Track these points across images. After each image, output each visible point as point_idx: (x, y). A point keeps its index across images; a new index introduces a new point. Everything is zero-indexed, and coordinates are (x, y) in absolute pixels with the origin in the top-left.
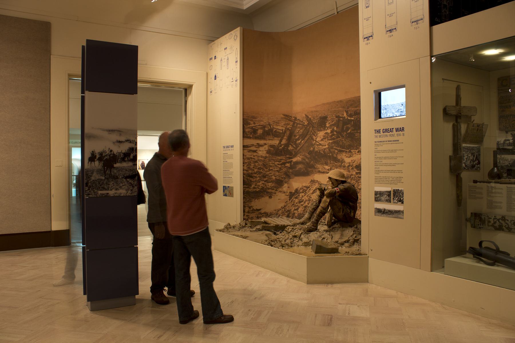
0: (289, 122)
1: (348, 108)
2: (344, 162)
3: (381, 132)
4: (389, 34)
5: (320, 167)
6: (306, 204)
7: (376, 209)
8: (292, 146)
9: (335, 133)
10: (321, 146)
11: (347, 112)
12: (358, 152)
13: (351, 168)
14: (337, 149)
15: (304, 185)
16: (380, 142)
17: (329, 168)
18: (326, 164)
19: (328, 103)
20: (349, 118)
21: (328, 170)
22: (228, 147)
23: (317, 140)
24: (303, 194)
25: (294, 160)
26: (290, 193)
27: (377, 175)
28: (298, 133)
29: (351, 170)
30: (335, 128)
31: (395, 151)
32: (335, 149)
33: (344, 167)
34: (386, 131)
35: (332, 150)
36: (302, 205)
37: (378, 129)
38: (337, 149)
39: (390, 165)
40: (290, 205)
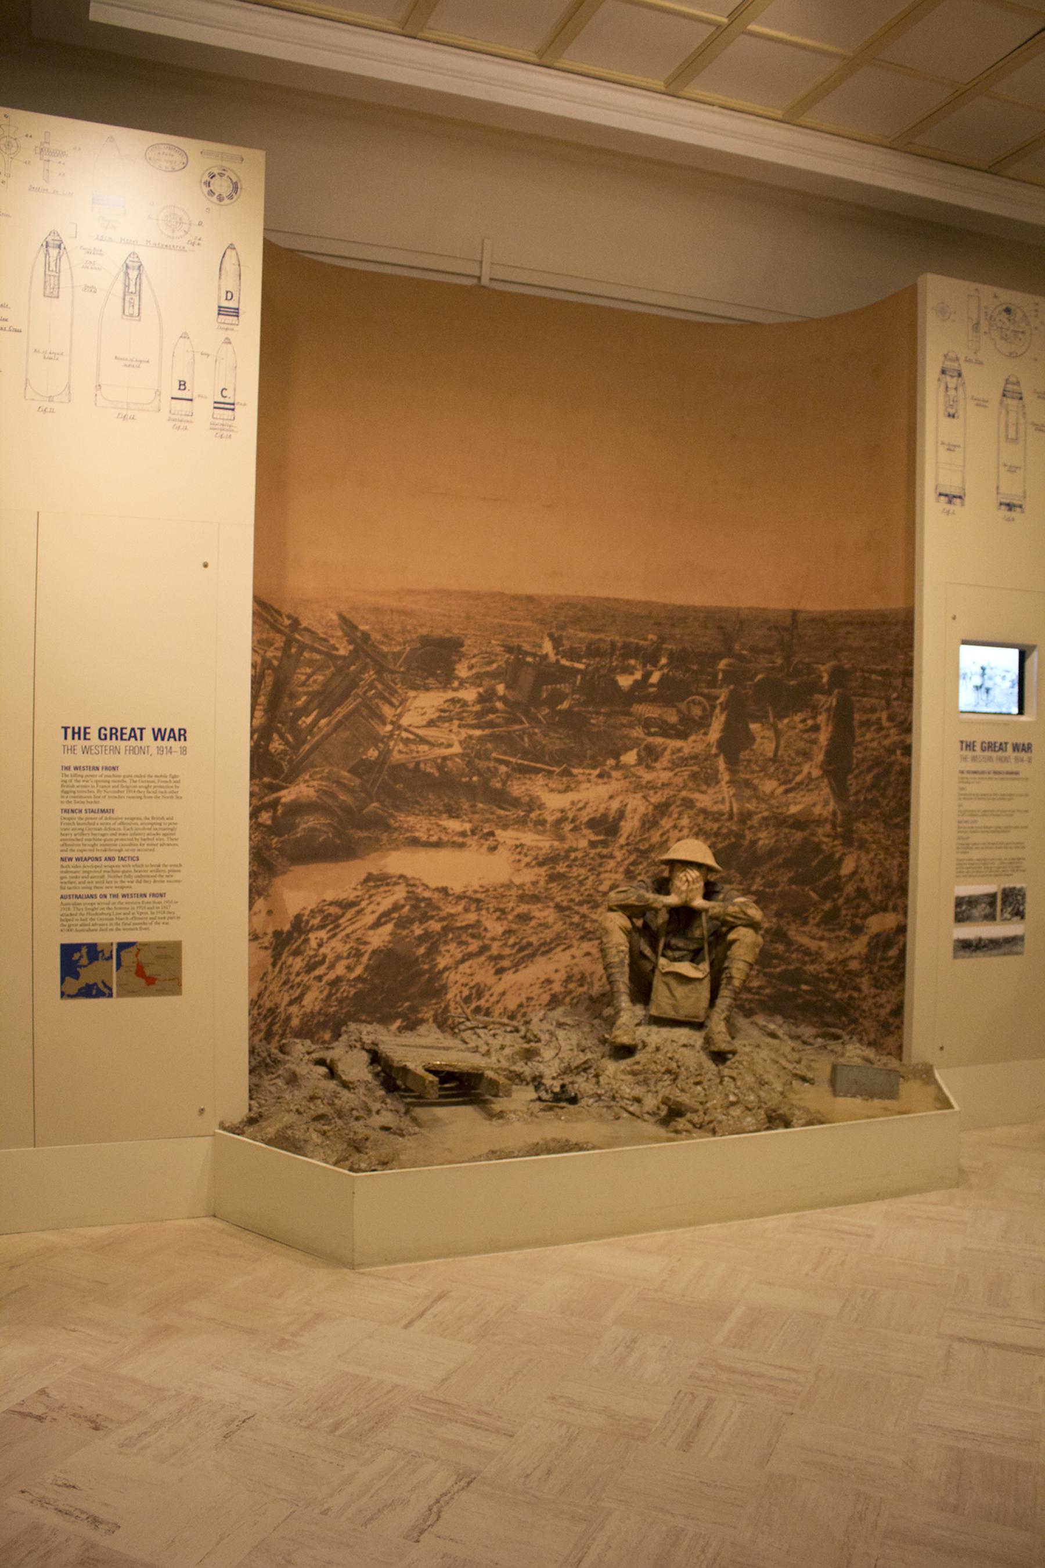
0: (273, 634)
1: (562, 627)
2: (541, 807)
3: (978, 747)
4: (1004, 511)
5: (420, 825)
6: (340, 970)
7: (958, 941)
8: (282, 737)
9: (499, 705)
10: (426, 748)
11: (557, 642)
12: (600, 776)
13: (567, 827)
14: (507, 763)
15: (330, 896)
16: (975, 772)
17: (467, 826)
18: (453, 813)
19: (467, 594)
20: (564, 662)
21: (463, 834)
22: (116, 733)
23: (404, 722)
24: (323, 934)
25: (288, 796)
26: (277, 934)
27: (961, 856)
28: (304, 684)
29: (569, 835)
30: (501, 689)
31: (1010, 797)
32: (500, 761)
33: (542, 822)
34: (990, 746)
35: (482, 764)
36: (319, 978)
37: (969, 739)
38: (507, 763)
39: (997, 830)
40: (274, 987)
